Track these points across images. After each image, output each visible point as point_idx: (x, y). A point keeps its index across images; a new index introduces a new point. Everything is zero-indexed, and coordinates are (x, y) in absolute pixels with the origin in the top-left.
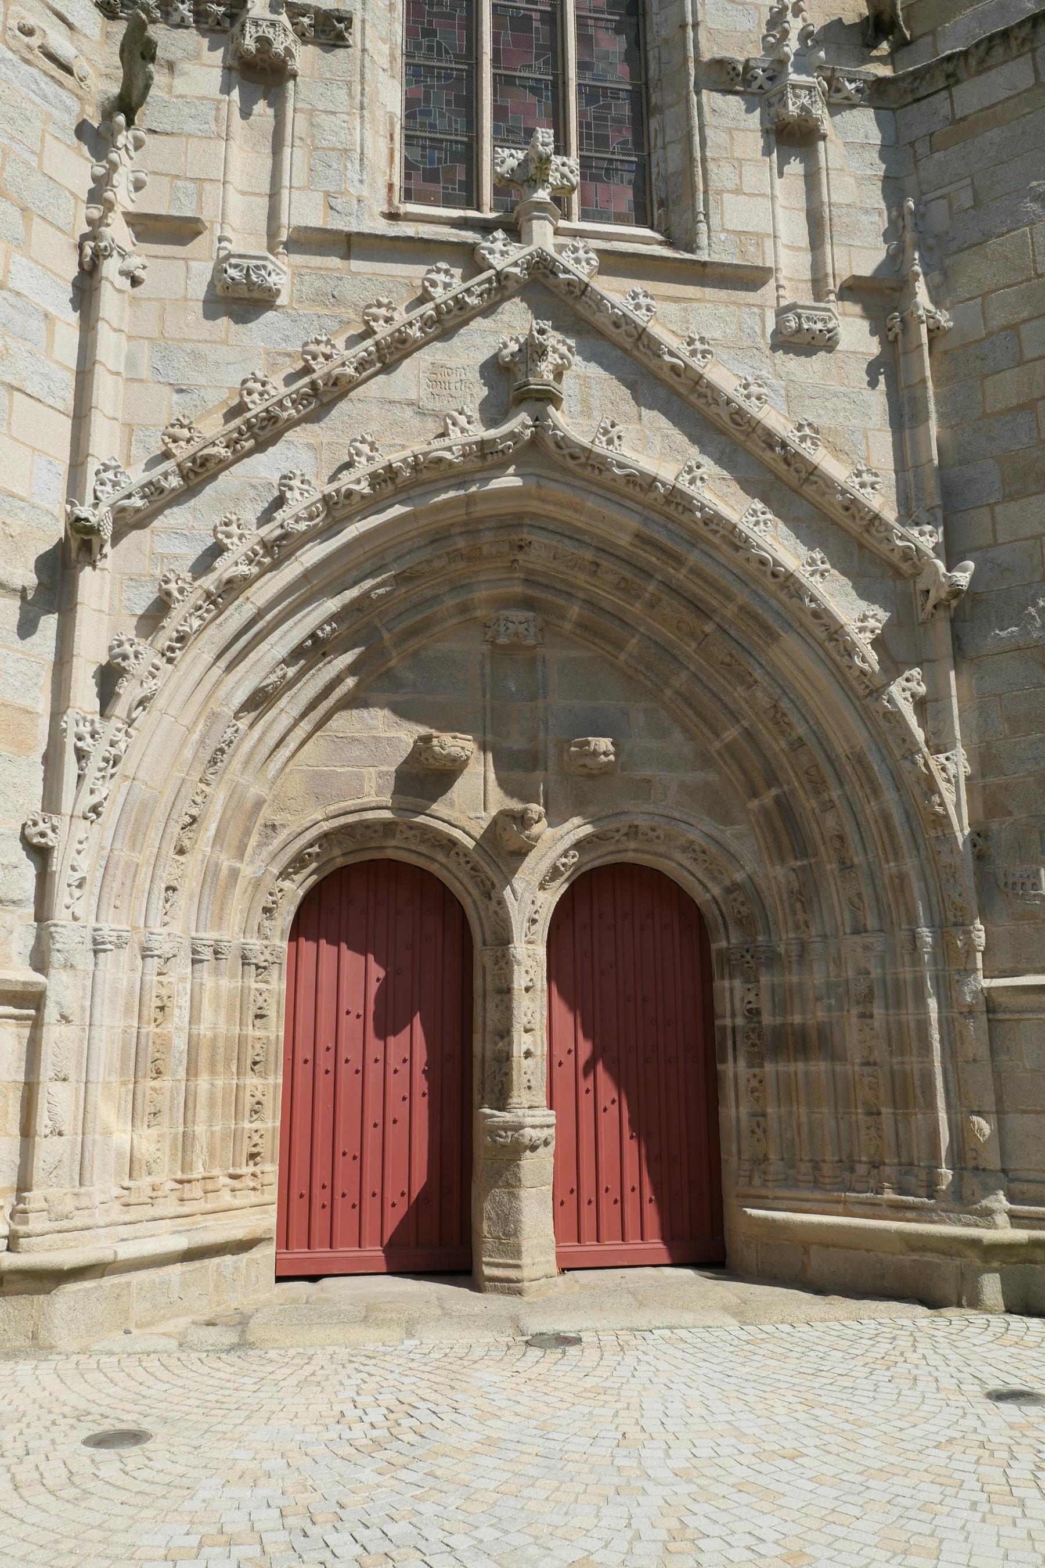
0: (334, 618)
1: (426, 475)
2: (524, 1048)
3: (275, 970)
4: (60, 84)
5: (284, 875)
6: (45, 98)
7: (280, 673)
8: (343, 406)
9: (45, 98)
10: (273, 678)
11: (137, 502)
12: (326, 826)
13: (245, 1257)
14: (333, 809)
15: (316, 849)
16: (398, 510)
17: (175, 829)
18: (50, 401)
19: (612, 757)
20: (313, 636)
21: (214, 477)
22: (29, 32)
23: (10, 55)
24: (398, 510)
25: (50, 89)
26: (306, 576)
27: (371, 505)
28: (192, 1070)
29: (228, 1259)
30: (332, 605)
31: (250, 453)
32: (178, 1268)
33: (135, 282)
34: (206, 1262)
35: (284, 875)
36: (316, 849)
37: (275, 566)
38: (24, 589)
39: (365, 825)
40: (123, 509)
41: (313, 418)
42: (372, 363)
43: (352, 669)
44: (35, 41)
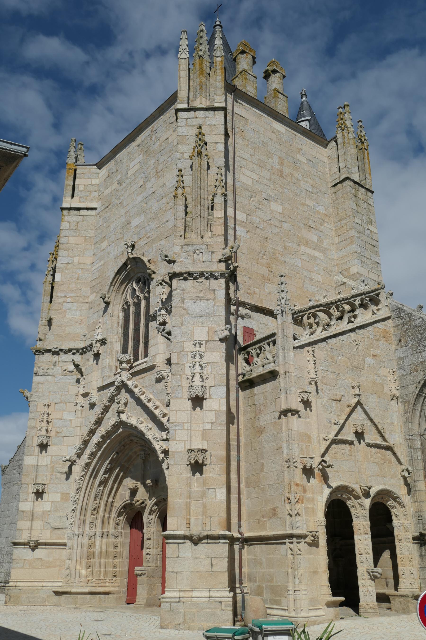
0: (109, 464)
1: (109, 434)
2: (146, 553)
3: (120, 537)
4: (72, 375)
5: (118, 516)
6: (69, 380)
7: (103, 477)
8: (103, 422)
9: (69, 380)
10: (102, 478)
11: (79, 451)
12: (122, 505)
13: (107, 596)
14: (123, 501)
15: (123, 510)
16: (108, 441)
17: (91, 511)
18: (71, 436)
19: (151, 484)
20: (107, 468)
21: (89, 442)
22: (65, 370)
23: (62, 377)
24: (108, 441)
25: (69, 377)
26: (100, 458)
27: (104, 442)
28: (100, 558)
29: (102, 596)
30: (108, 462)
31: (92, 436)
32: (89, 596)
33: (83, 407)
34: (96, 595)
35: (118, 516)
36: (123, 510)
37: (94, 458)
38: (66, 472)
39: (126, 504)
40: (77, 453)
41: (99, 426)
42: (104, 412)
43: (120, 471)
44: (66, 371)
